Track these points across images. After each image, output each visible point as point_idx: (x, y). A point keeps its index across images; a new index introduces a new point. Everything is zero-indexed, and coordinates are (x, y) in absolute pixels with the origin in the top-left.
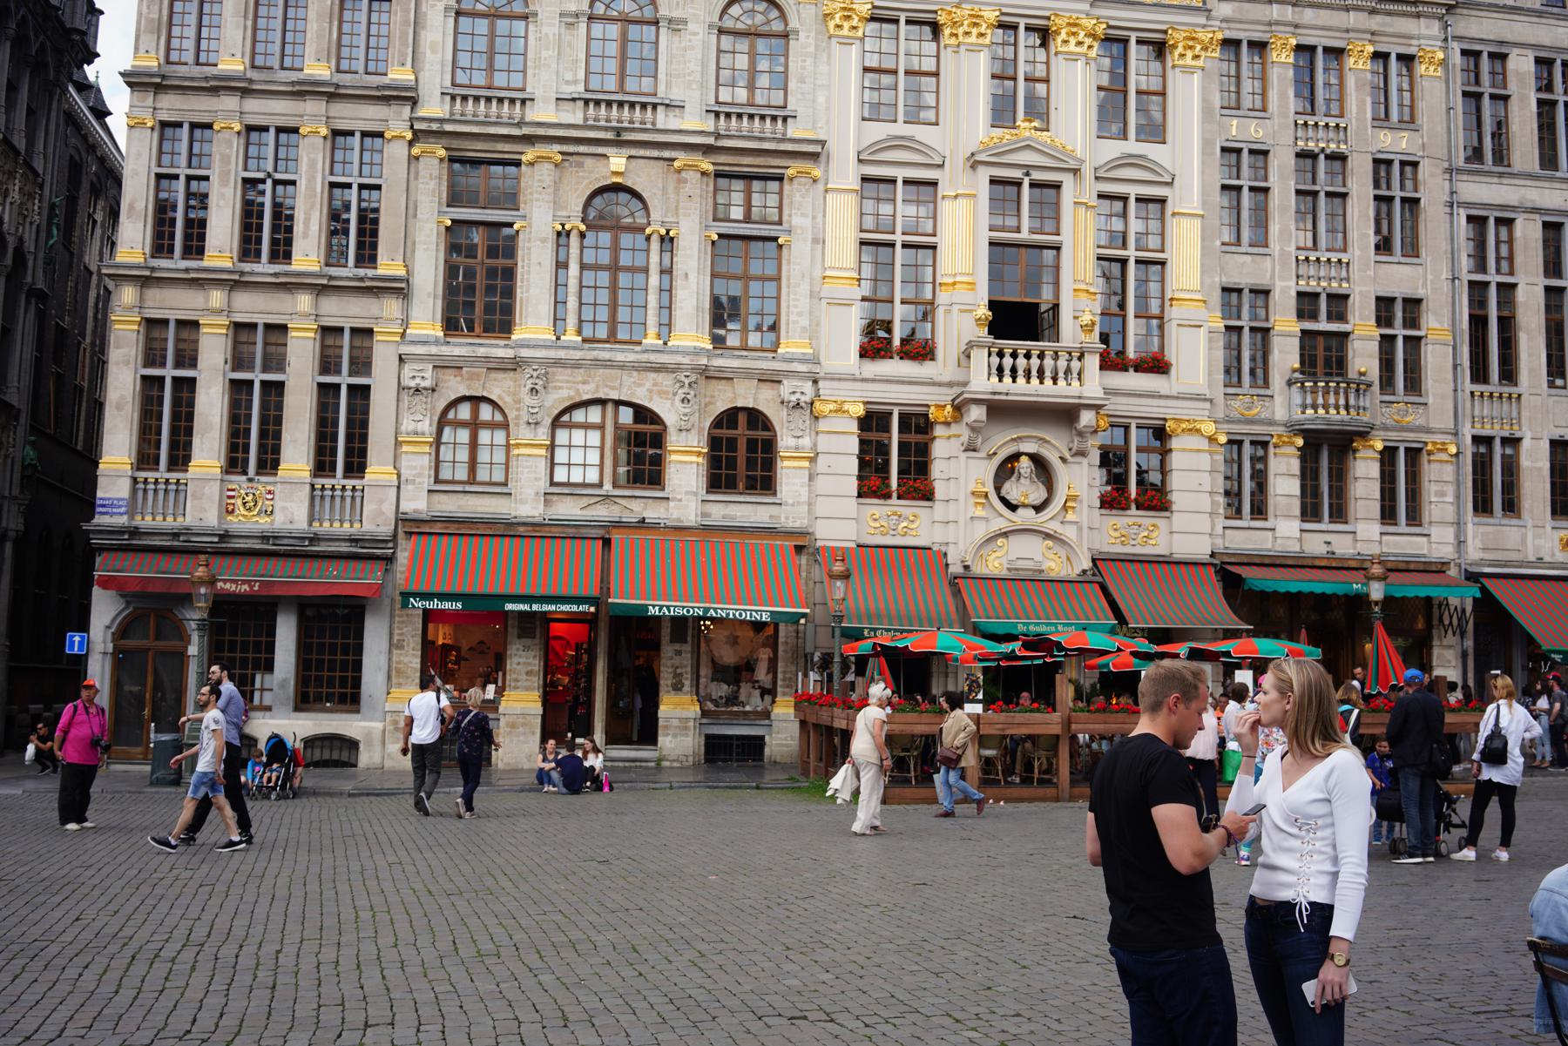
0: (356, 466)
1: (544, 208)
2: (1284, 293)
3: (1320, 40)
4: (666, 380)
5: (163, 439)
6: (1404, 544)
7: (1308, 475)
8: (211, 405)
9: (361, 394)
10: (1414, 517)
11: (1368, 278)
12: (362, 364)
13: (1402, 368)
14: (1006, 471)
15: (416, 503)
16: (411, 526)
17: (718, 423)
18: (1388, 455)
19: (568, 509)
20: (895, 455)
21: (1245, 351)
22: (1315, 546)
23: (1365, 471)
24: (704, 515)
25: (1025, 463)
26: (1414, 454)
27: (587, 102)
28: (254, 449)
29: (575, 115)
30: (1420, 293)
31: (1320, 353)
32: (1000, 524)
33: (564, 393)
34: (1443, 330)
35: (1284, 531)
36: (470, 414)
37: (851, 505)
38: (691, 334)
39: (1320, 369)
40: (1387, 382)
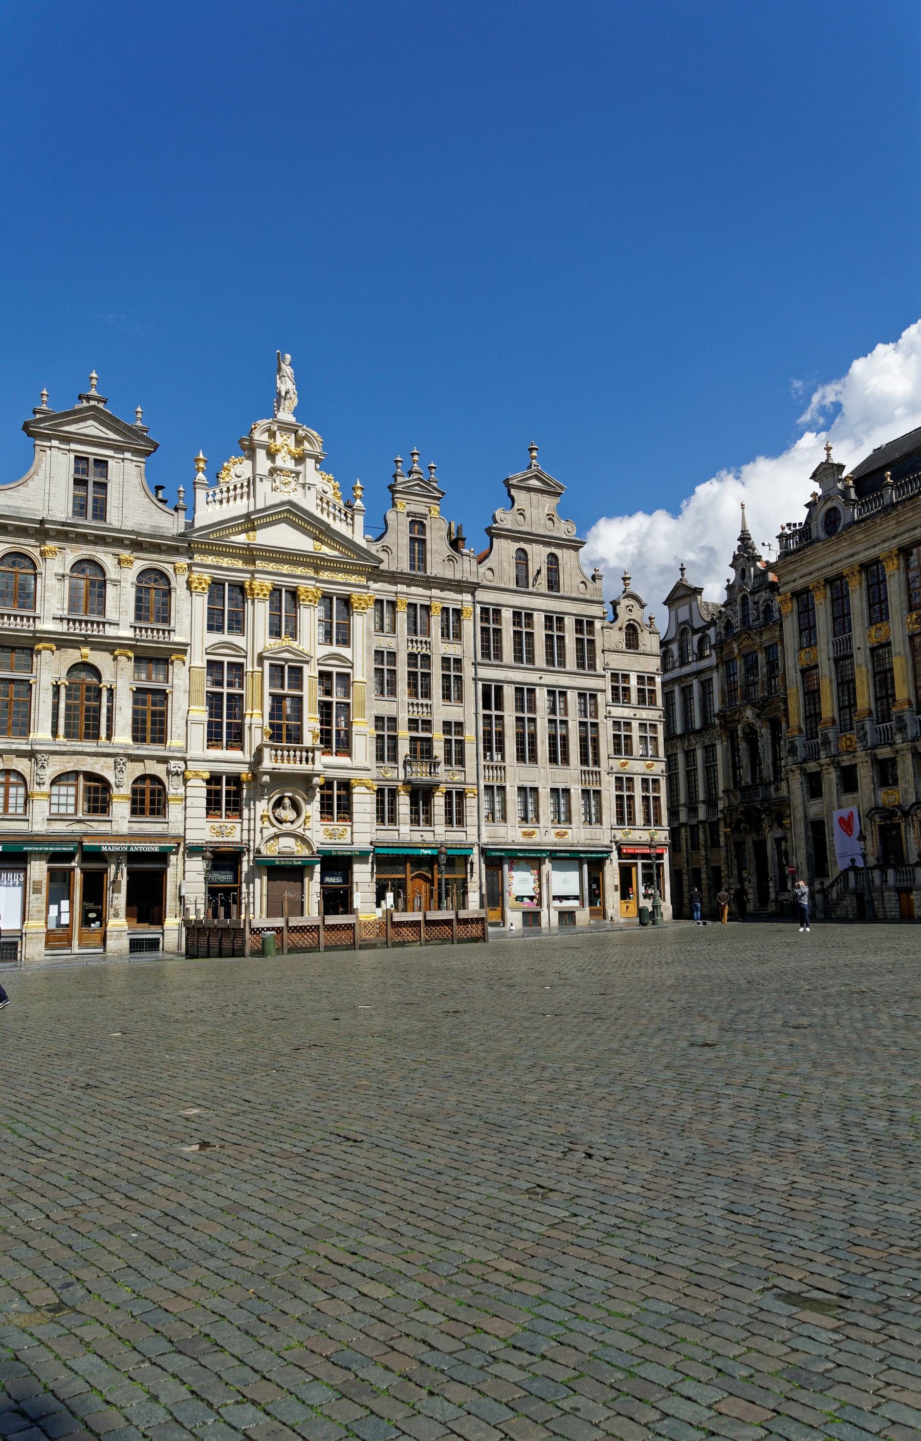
3: (419, 602)
4: (111, 761)
6: (455, 836)
7: (414, 803)
10: (460, 822)
11: (442, 711)
14: (279, 804)
17: (135, 782)
18: (448, 794)
20: (226, 795)
21: (386, 749)
22: (416, 837)
23: (439, 801)
24: (130, 828)
25: (287, 801)
26: (461, 795)
27: (69, 620)
29: (61, 627)
30: (461, 720)
31: (419, 747)
33: (58, 768)
34: (471, 736)
35: (405, 832)
38: (123, 737)
39: (419, 755)
40: (448, 761)
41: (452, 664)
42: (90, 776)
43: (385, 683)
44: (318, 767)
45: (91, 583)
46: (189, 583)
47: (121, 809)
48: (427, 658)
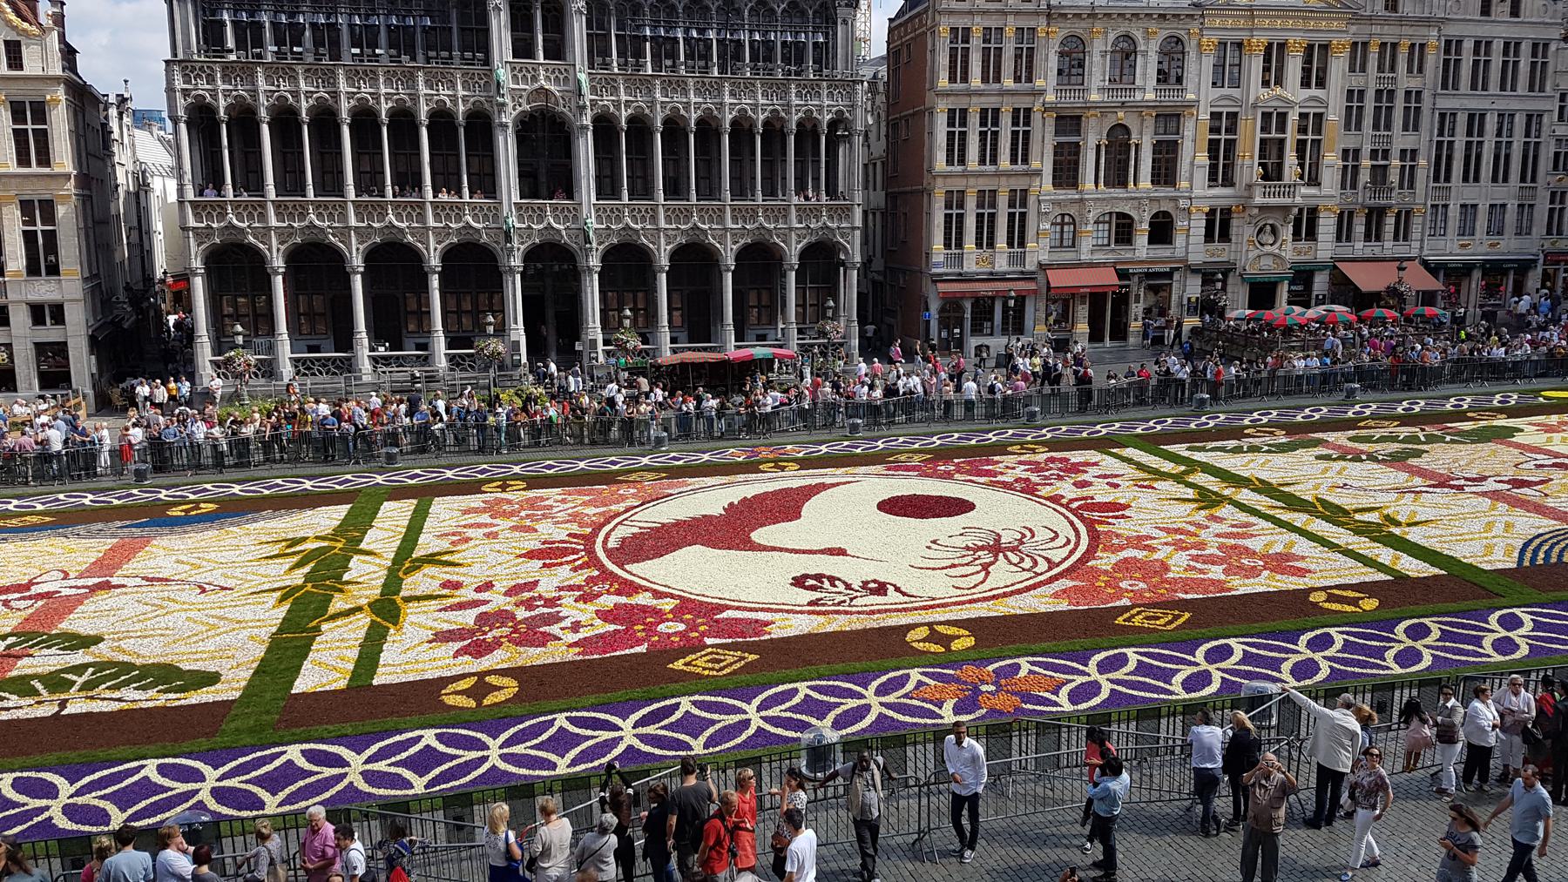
0: (1022, 244)
1: (1093, 137)
2: (1367, 149)
4: (1136, 203)
5: (954, 236)
8: (970, 224)
9: (1023, 215)
10: (1405, 239)
11: (1401, 140)
12: (1024, 204)
13: (1409, 177)
15: (1044, 257)
16: (1042, 267)
18: (1398, 215)
19: (1099, 257)
20: (1219, 226)
21: (1349, 176)
23: (1390, 221)
26: (1408, 213)
28: (986, 239)
32: (1257, 252)
36: (1068, 226)
37: (1202, 247)
38: (1145, 183)
41: (1414, 96)
42: (1121, 216)
43: (1352, 119)
44: (1298, 200)
45: (1126, 54)
46: (1199, 45)
47: (1141, 240)
48: (1391, 93)
